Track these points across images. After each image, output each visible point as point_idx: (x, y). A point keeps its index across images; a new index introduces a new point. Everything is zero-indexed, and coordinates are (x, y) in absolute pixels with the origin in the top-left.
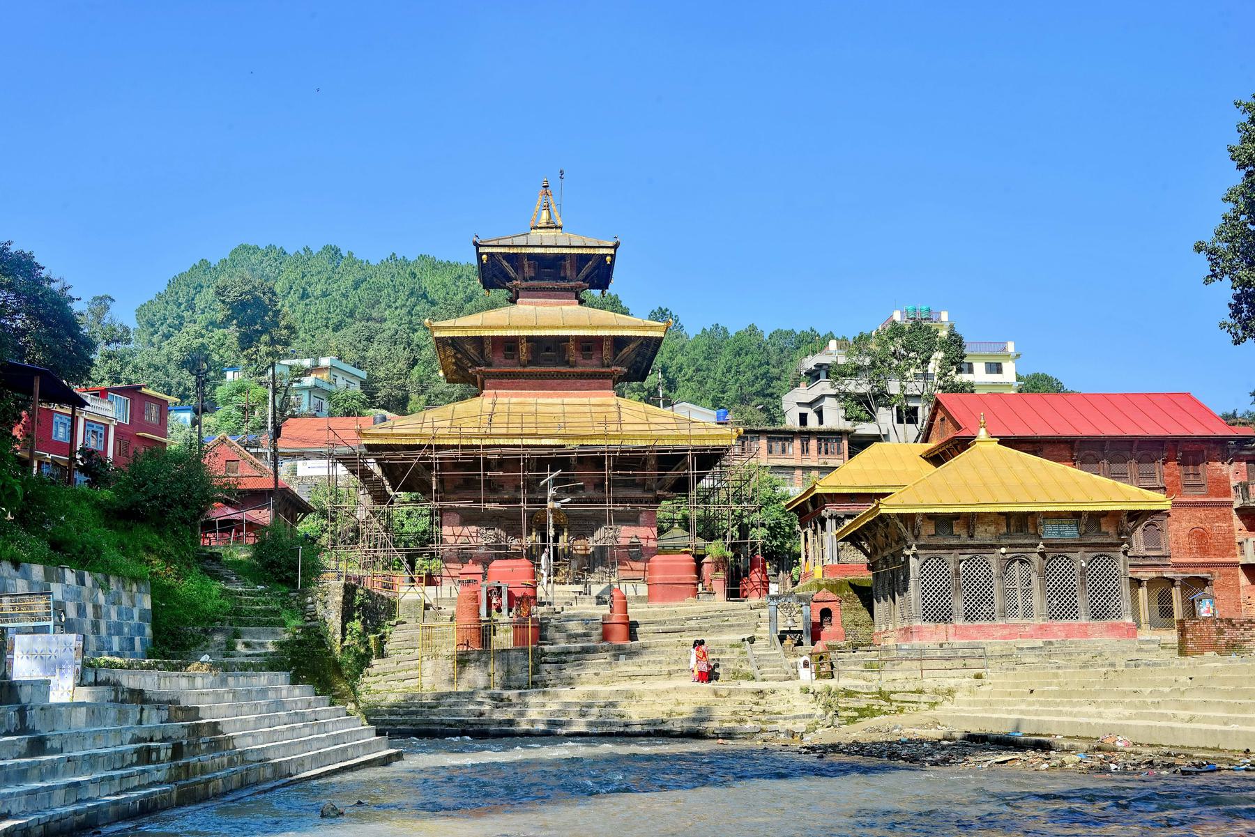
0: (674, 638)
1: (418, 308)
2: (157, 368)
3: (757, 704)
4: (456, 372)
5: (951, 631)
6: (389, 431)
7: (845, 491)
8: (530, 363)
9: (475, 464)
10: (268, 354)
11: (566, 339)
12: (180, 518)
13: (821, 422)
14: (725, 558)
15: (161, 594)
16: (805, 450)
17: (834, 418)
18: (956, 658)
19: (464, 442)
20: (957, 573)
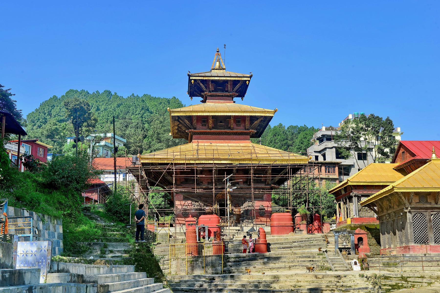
0: (288, 251)
1: (145, 115)
3: (338, 282)
4: (177, 133)
5: (429, 248)
6: (153, 157)
7: (362, 184)
8: (213, 128)
9: (192, 172)
10: (86, 131)
11: (230, 117)
12: (76, 188)
13: (325, 159)
14: (306, 214)
15: (65, 227)
16: (320, 171)
17: (331, 157)
18: (434, 261)
19: (187, 162)
20: (430, 221)
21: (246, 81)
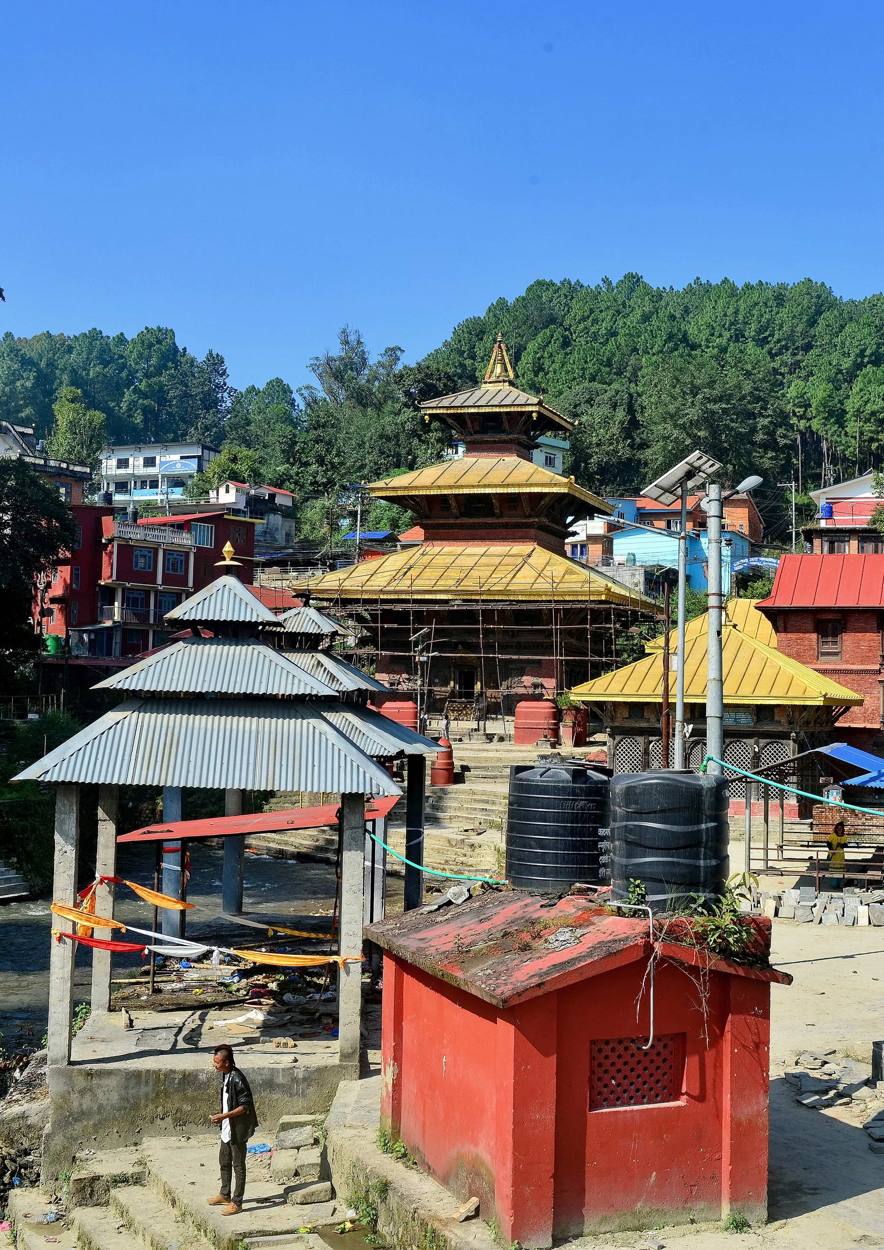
2: (389, 439)
8: (463, 515)
21: (533, 412)
